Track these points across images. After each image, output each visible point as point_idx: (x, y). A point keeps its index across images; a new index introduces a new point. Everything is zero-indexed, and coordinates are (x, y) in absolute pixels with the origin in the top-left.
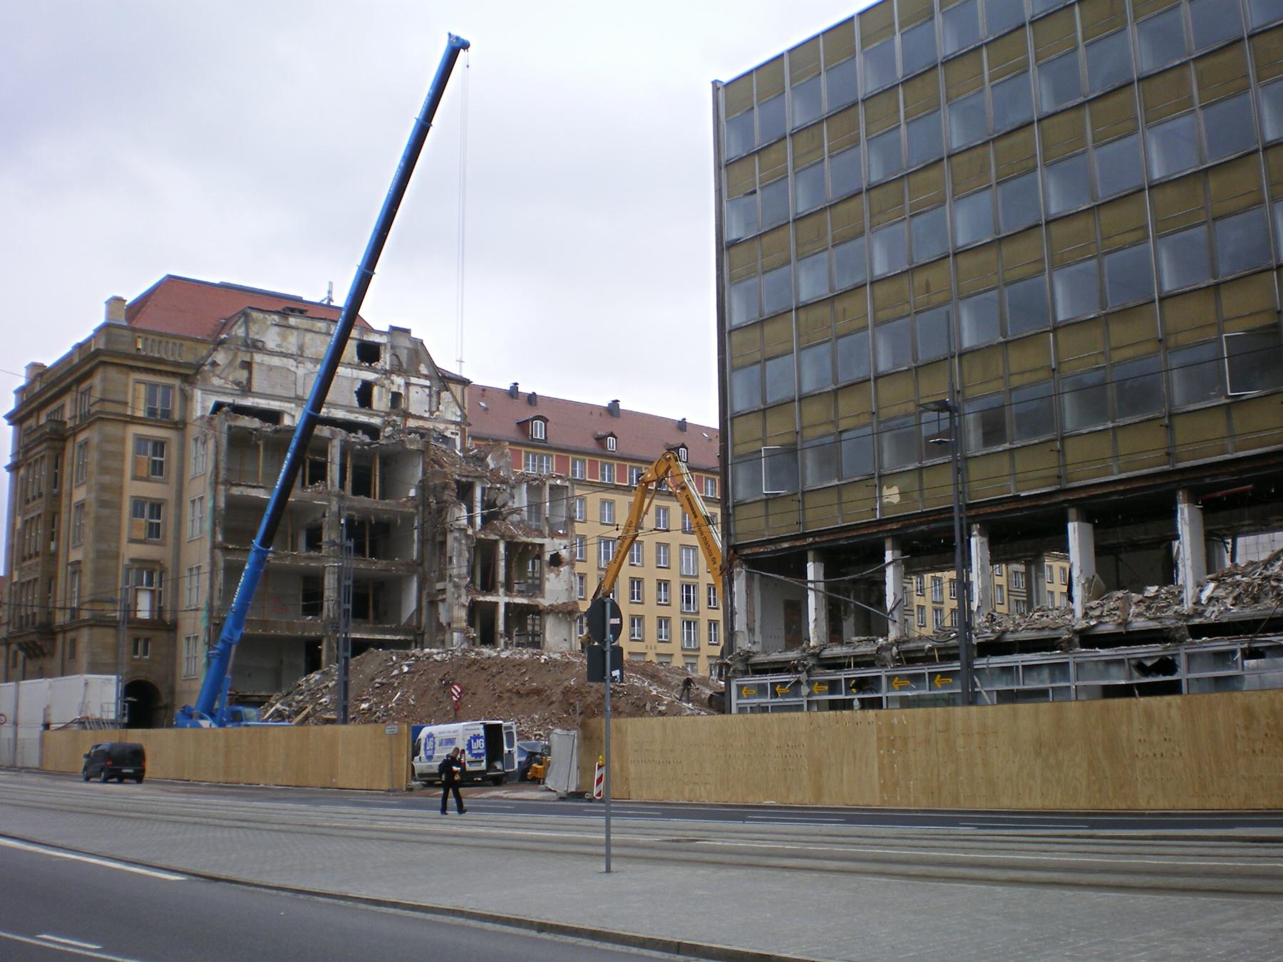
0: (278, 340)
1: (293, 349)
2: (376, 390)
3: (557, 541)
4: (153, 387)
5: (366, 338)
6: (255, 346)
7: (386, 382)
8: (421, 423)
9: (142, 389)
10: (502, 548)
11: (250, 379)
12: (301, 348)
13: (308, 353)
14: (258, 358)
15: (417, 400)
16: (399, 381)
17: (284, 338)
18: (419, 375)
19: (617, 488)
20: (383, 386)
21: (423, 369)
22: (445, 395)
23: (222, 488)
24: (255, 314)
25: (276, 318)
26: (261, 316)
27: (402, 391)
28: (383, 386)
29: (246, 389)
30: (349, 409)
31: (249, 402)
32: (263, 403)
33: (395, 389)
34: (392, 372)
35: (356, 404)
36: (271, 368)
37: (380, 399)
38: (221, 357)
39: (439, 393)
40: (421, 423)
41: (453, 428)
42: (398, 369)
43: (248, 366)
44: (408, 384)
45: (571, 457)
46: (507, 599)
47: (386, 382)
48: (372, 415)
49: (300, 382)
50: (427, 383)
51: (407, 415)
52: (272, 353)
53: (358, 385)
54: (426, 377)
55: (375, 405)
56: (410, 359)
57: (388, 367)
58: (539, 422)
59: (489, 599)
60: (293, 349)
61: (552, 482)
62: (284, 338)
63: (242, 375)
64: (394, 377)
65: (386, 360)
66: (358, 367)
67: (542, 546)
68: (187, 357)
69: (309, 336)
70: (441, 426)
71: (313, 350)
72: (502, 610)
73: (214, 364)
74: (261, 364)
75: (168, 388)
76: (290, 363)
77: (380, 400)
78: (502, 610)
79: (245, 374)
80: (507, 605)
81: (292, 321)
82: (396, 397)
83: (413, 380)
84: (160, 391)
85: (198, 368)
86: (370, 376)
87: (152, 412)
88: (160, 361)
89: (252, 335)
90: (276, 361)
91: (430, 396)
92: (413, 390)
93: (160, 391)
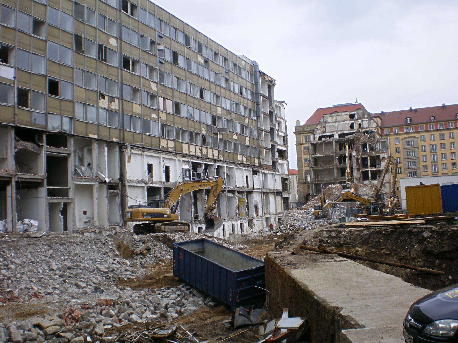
0: (331, 120)
1: (334, 121)
2: (354, 124)
3: (383, 154)
4: (306, 136)
5: (351, 113)
6: (326, 122)
7: (357, 122)
8: (366, 129)
9: (304, 137)
10: (369, 158)
11: (325, 130)
12: (336, 120)
13: (338, 120)
14: (327, 125)
15: (365, 124)
16: (360, 121)
17: (332, 119)
18: (365, 118)
19: (434, 131)
20: (356, 123)
21: (366, 116)
22: (372, 121)
23: (310, 156)
24: (325, 116)
25: (329, 115)
26: (326, 115)
27: (361, 123)
28: (356, 123)
29: (325, 132)
30: (348, 130)
31: (326, 134)
32: (329, 134)
33: (359, 123)
34: (358, 119)
35: (350, 129)
36: (330, 126)
37: (356, 126)
38: (319, 127)
39: (370, 121)
40: (366, 129)
41: (375, 128)
42: (359, 118)
43: (325, 127)
44: (362, 121)
45: (419, 125)
46: (371, 169)
47: (357, 122)
48: (354, 130)
49: (336, 127)
50: (367, 119)
51: (363, 128)
52: (330, 123)
53: (350, 124)
54: (367, 118)
55: (355, 128)
56: (362, 115)
57: (357, 118)
59: (366, 170)
60: (334, 121)
61: (381, 140)
62: (332, 119)
63: (324, 129)
65: (356, 117)
66: (350, 120)
67: (380, 156)
68: (312, 129)
69: (338, 117)
70: (371, 129)
71: (339, 119)
72: (370, 172)
73: (317, 129)
74: (327, 126)
76: (334, 124)
77: (356, 126)
78: (370, 172)
80: (368, 171)
81: (333, 115)
82: (360, 125)
83: (364, 120)
84: (307, 137)
85: (314, 130)
86: (353, 122)
87: (306, 141)
88: (305, 131)
89: (325, 120)
90: (331, 124)
91: (368, 122)
92: (364, 122)
93: (307, 137)
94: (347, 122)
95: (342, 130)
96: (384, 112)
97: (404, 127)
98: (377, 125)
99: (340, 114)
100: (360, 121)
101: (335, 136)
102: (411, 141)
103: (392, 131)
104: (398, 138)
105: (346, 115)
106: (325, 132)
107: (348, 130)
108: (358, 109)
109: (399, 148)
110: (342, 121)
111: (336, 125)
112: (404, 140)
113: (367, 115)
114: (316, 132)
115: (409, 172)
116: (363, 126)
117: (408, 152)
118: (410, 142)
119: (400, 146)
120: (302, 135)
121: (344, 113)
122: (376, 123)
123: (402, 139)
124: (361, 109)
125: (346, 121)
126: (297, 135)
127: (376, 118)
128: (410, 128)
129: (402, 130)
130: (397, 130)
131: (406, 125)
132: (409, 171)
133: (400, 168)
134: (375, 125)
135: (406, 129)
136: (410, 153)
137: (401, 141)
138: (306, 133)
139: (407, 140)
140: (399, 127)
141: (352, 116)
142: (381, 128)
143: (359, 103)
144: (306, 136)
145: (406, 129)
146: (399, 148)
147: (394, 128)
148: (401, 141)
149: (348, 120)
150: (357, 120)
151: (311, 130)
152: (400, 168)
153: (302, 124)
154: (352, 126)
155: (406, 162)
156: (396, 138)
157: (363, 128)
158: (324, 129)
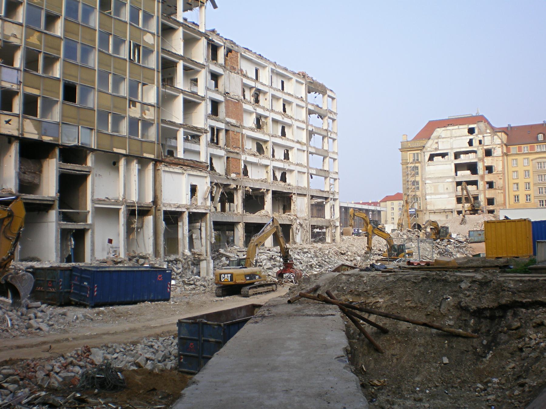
2: (474, 141)
9: (412, 156)
14: (440, 140)
18: (487, 133)
21: (488, 131)
22: (495, 137)
27: (482, 139)
30: (466, 148)
33: (480, 139)
35: (468, 146)
36: (443, 142)
39: (493, 137)
42: (480, 133)
43: (437, 143)
44: (483, 137)
50: (490, 135)
52: (443, 138)
53: (468, 140)
54: (489, 133)
58: (541, 135)
60: (449, 135)
64: (479, 136)
75: (417, 154)
76: (449, 139)
77: (476, 143)
79: (437, 145)
82: (480, 142)
83: (485, 135)
85: (424, 147)
87: (414, 160)
88: (413, 148)
90: (444, 140)
92: (485, 137)
94: (465, 137)
95: (458, 147)
96: (512, 126)
97: (535, 144)
98: (502, 142)
99: (456, 127)
100: (480, 137)
101: (449, 154)
102: (544, 162)
103: (520, 149)
104: (528, 159)
105: (464, 129)
106: (437, 149)
107: (466, 148)
108: (478, 122)
109: (528, 171)
110: (459, 137)
111: (452, 140)
112: (534, 161)
113: (490, 130)
114: (426, 150)
115: (540, 201)
116: (484, 143)
117: (539, 175)
118: (543, 164)
119: (530, 168)
120: (409, 152)
121: (461, 127)
122: (501, 139)
123: (532, 160)
124: (482, 121)
125: (463, 136)
126: (403, 152)
127: (500, 133)
128: (543, 147)
129: (532, 148)
130: (525, 148)
131: (537, 141)
132: (540, 199)
133: (529, 196)
134: (498, 141)
135: (538, 147)
136: (541, 177)
137: (531, 163)
138: (414, 150)
139: (539, 160)
140: (529, 145)
141: (471, 131)
142: (506, 145)
143: (480, 114)
144: (414, 154)
145: (538, 147)
146: (528, 171)
147: (522, 146)
148: (531, 163)
149: (466, 136)
150: (477, 135)
151: (420, 147)
152: (529, 196)
153: (410, 139)
154: (470, 143)
155: (536, 188)
156: (525, 159)
157: (484, 145)
158: (436, 146)
